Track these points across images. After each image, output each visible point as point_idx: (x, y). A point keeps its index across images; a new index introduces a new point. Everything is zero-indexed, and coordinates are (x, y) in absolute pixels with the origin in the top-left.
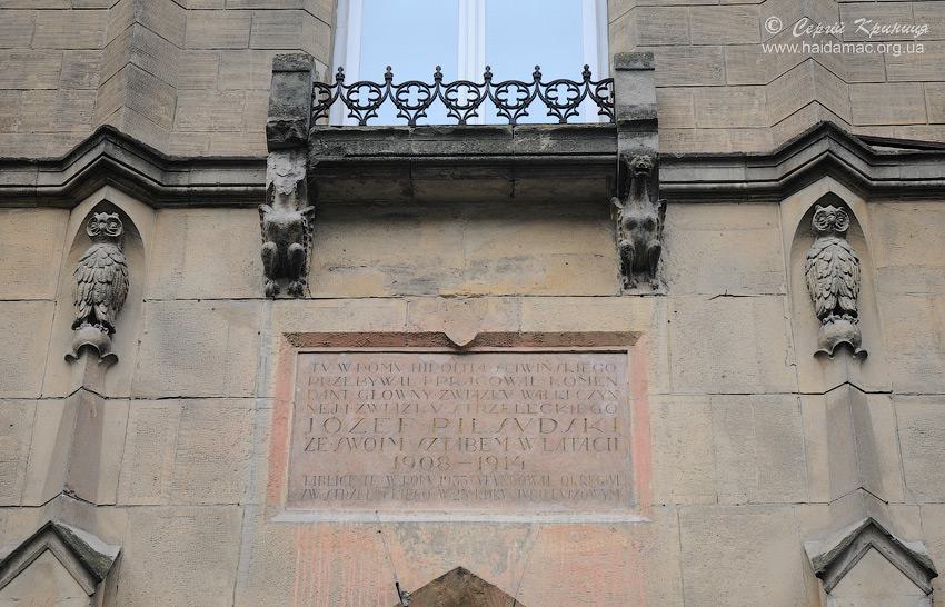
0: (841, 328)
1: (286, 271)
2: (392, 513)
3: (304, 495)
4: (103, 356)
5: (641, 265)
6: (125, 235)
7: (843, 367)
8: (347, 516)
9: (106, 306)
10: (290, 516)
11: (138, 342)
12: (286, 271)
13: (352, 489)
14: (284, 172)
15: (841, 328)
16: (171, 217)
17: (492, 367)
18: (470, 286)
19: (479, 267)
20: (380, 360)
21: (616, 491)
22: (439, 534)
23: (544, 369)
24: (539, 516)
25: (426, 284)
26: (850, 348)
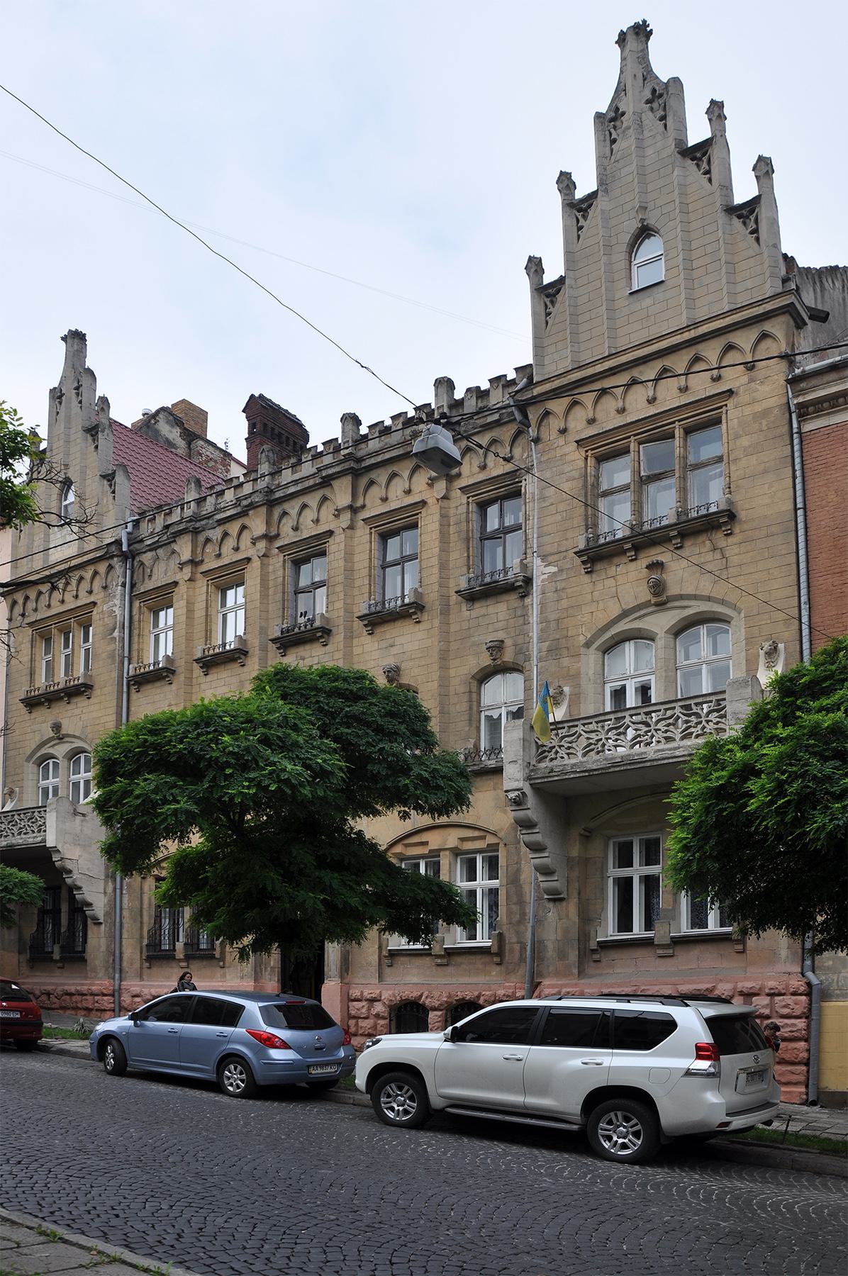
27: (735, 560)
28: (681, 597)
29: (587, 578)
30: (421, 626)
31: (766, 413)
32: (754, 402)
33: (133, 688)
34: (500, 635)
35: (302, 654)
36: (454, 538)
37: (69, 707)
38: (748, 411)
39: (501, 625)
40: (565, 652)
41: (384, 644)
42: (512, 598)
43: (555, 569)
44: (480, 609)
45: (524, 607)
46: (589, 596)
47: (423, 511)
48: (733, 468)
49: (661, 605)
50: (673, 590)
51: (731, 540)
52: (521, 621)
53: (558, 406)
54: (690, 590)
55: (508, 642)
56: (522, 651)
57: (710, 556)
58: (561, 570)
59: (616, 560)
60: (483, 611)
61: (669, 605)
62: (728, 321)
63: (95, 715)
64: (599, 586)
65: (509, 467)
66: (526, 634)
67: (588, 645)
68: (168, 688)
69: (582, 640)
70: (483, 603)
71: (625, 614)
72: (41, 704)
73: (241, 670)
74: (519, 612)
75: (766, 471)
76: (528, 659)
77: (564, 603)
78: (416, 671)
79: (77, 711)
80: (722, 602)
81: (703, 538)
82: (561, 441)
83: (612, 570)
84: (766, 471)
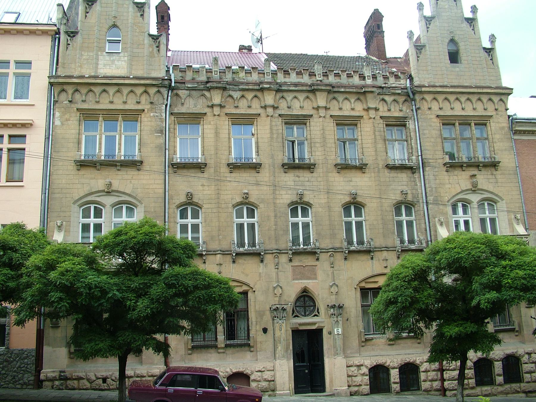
1: (291, 260)
2: (300, 281)
3: (293, 280)
5: (318, 259)
7: (332, 269)
8: (297, 282)
9: (277, 264)
10: (293, 281)
11: (280, 268)
12: (291, 260)
13: (297, 279)
14: (290, 252)
17: (306, 268)
21: (316, 279)
22: (304, 283)
24: (310, 281)
25: (301, 261)
27: (500, 180)
28: (482, 190)
29: (446, 173)
30: (365, 175)
31: (502, 128)
32: (498, 123)
34: (405, 188)
36: (378, 137)
37: (119, 173)
38: (497, 125)
39: (405, 183)
41: (346, 179)
42: (409, 172)
44: (394, 174)
45: (415, 178)
46: (448, 181)
47: (361, 120)
49: (474, 191)
50: (480, 186)
51: (497, 172)
53: (429, 97)
54: (485, 188)
55: (409, 192)
57: (490, 177)
59: (457, 169)
60: (395, 175)
61: (477, 192)
62: (492, 91)
63: (144, 182)
64: (451, 178)
65: (401, 114)
66: (417, 190)
67: (448, 201)
69: (446, 199)
70: (396, 171)
71: (462, 191)
73: (257, 175)
74: (412, 179)
75: (505, 150)
79: (130, 177)
80: (497, 195)
81: (488, 169)
82: (429, 112)
83: (456, 172)
84: (505, 150)
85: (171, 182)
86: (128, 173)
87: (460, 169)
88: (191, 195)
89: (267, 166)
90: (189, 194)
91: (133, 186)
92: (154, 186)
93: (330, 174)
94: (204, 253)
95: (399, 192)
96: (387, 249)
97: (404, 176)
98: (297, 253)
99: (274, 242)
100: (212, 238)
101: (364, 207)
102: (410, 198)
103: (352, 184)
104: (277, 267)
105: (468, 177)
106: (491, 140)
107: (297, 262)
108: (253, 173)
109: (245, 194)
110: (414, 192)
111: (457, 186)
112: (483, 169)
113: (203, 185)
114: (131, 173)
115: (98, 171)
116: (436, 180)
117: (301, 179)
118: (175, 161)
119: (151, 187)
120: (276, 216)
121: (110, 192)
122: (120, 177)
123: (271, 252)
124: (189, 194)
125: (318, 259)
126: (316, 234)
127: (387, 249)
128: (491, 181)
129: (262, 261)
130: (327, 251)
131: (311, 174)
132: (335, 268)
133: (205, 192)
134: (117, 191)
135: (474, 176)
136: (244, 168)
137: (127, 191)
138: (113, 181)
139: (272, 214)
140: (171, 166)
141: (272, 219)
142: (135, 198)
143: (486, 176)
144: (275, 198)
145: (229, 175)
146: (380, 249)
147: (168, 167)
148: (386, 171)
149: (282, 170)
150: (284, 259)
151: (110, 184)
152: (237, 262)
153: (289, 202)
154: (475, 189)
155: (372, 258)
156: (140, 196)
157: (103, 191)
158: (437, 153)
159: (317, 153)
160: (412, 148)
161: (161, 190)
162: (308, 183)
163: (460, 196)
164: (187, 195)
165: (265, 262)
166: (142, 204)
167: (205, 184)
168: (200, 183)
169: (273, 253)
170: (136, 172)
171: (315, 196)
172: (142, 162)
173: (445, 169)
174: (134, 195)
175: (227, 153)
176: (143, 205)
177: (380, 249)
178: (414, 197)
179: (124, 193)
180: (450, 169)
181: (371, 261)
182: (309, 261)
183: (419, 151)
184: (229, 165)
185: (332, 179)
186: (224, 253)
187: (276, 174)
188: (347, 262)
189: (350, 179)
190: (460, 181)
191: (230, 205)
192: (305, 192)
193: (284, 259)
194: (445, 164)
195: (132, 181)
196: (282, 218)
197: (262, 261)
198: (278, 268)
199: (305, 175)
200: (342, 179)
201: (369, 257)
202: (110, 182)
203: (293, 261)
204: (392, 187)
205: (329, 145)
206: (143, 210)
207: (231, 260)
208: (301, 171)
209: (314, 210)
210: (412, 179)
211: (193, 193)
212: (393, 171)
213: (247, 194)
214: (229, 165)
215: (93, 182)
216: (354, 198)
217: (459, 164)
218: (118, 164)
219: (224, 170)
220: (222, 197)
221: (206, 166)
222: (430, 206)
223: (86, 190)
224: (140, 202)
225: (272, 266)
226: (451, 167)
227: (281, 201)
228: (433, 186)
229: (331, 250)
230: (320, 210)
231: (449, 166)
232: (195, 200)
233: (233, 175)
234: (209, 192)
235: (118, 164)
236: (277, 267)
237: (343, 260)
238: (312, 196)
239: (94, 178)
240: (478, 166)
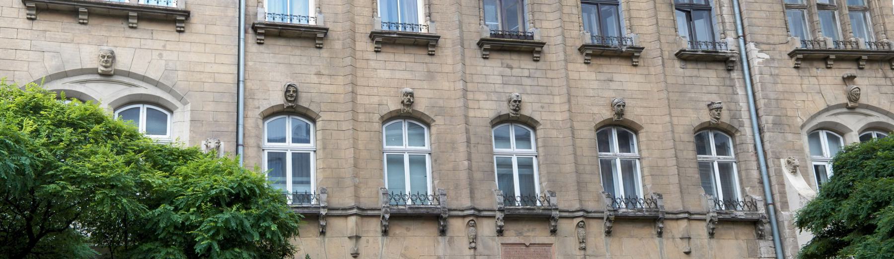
0: (583, 245)
4: (475, 248)
5: (554, 232)
6: (474, 226)
7: (582, 252)
9: (474, 239)
11: (480, 248)
12: (500, 232)
14: (499, 215)
15: (583, 245)
16: (480, 219)
17: (532, 249)
18: (528, 234)
19: (529, 230)
20: (515, 247)
23: (539, 249)
26: (584, 249)
28: (867, 107)
29: (794, 71)
33: (251, 38)
34: (715, 99)
35: (510, 62)
37: (133, 33)
39: (713, 89)
40: (787, 128)
41: (602, 77)
42: (721, 68)
43: (767, 57)
44: (691, 70)
45: (732, 79)
46: (799, 87)
48: (886, 20)
49: (851, 110)
50: (863, 100)
52: (730, 90)
54: (874, 103)
56: (735, 116)
57: (882, 81)
58: (773, 59)
59: (816, 64)
60: (695, 72)
61: (858, 110)
63: (194, 57)
66: (737, 103)
67: (802, 127)
68: (316, 52)
69: (799, 122)
70: (694, 66)
71: (828, 109)
72: (126, 18)
73: (428, 59)
76: (742, 125)
77: (780, 87)
78: (639, 111)
79: (157, 45)
81: (876, 66)
83: (814, 71)
85: (250, 63)
86: (155, 36)
87: (822, 65)
88: (296, 91)
89: (449, 43)
90: (292, 89)
91: (167, 64)
92: (216, 68)
93: (571, 66)
94: (323, 212)
95: (704, 105)
96: (690, 217)
97: (711, 76)
98: (512, 218)
99: (465, 193)
100: (339, 182)
101: (636, 133)
102: (725, 118)
103: (613, 85)
104: (473, 245)
105: (839, 80)
106: (877, 11)
107: (511, 236)
108: (421, 55)
109: (407, 94)
110: (733, 107)
111: (818, 98)
112: (867, 67)
113: (319, 74)
114: (164, 35)
115: (83, 27)
116: (775, 83)
117: (516, 72)
118: (260, 19)
119: (208, 69)
120: (468, 141)
121: (111, 75)
122: (135, 43)
123: (460, 213)
124: (292, 89)
125: (554, 232)
126: (549, 181)
127: (690, 217)
128: (884, 89)
129: (443, 232)
130: (571, 215)
131: (535, 63)
132: (589, 252)
133: (323, 88)
134: (128, 74)
135: (850, 79)
136: (404, 45)
137: (152, 75)
138: (117, 52)
139: (461, 138)
140: (250, 31)
141: (462, 148)
142: (170, 91)
143: (873, 81)
144: (467, 107)
145: (373, 56)
146: (675, 217)
147: (246, 32)
148: (678, 64)
149: (479, 53)
150: (487, 228)
151: (111, 58)
152: (391, 233)
153: (492, 115)
154: (853, 105)
155: (660, 234)
156: (181, 87)
157: (94, 71)
158: (774, 31)
159: (546, 24)
160: (723, 23)
161: (230, 76)
162: (527, 81)
163: (825, 118)
164: (287, 91)
165: (449, 233)
166: (185, 104)
167: (323, 72)
168: (314, 70)
169: (464, 217)
170: (175, 36)
171: (542, 107)
172: (187, 14)
173: (792, 63)
174: (168, 83)
175: (367, 12)
176: (189, 107)
177: (675, 217)
178: (733, 117)
179: (144, 79)
180: (803, 65)
181: (657, 240)
182: (538, 235)
183: (739, 27)
184: (373, 36)
185: (573, 75)
186: (363, 214)
187: (467, 61)
188: (609, 240)
189: (609, 76)
190: (822, 87)
191: (376, 117)
192: (524, 98)
193: (487, 228)
194: (791, 55)
195: (165, 54)
196: (480, 147)
197: (443, 232)
198: (475, 248)
199: (522, 65)
200: (593, 76)
201: (654, 232)
202: (112, 53)
203: (506, 233)
204: (689, 95)
205: (566, 10)
206: (188, 116)
207: (379, 229)
208: (515, 57)
209: (540, 132)
210: (728, 82)
211: (300, 89)
212: (689, 66)
213: (411, 94)
214: (373, 36)
215: (68, 50)
216: (620, 114)
217: (822, 55)
218: (131, 14)
219: (365, 46)
220: (360, 99)
221: (326, 34)
222: (767, 136)
223: (51, 65)
224: (181, 99)
225: (463, 243)
226: (804, 59)
227: (478, 114)
228: (772, 96)
229: (581, 213)
230: (554, 133)
231: (800, 56)
232: (303, 102)
233: (381, 56)
234: (332, 89)
235: (131, 14)
236: (473, 245)
237: (604, 235)
238: (536, 106)
239: (72, 41)
240: (857, 60)
